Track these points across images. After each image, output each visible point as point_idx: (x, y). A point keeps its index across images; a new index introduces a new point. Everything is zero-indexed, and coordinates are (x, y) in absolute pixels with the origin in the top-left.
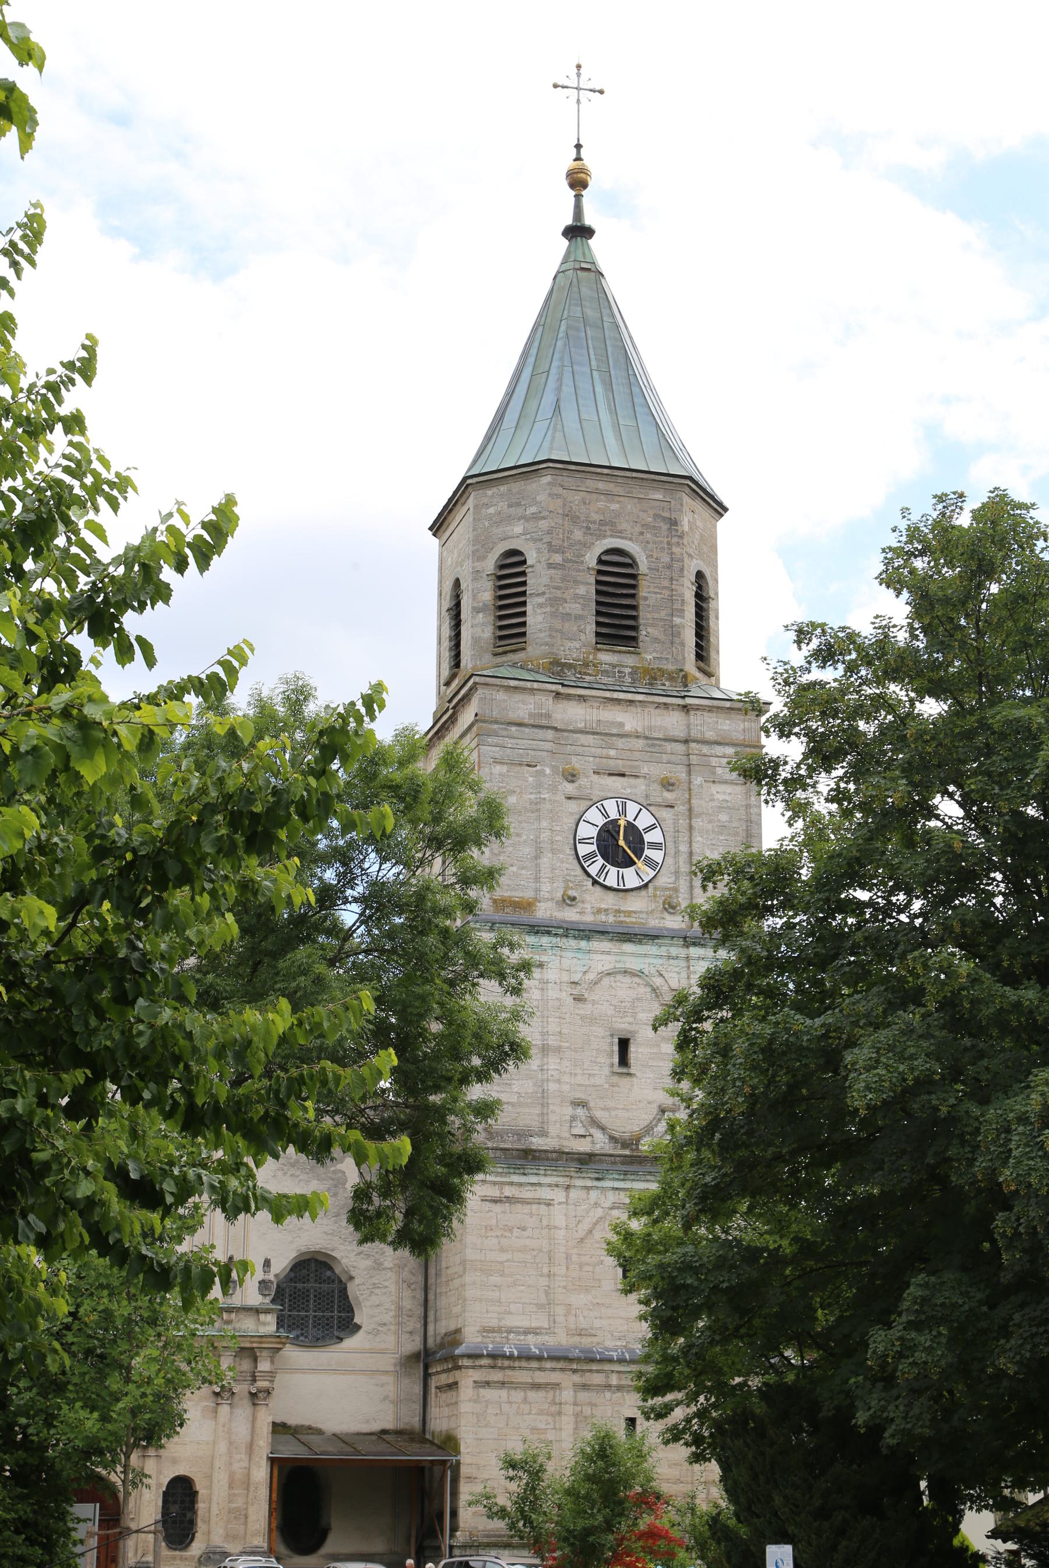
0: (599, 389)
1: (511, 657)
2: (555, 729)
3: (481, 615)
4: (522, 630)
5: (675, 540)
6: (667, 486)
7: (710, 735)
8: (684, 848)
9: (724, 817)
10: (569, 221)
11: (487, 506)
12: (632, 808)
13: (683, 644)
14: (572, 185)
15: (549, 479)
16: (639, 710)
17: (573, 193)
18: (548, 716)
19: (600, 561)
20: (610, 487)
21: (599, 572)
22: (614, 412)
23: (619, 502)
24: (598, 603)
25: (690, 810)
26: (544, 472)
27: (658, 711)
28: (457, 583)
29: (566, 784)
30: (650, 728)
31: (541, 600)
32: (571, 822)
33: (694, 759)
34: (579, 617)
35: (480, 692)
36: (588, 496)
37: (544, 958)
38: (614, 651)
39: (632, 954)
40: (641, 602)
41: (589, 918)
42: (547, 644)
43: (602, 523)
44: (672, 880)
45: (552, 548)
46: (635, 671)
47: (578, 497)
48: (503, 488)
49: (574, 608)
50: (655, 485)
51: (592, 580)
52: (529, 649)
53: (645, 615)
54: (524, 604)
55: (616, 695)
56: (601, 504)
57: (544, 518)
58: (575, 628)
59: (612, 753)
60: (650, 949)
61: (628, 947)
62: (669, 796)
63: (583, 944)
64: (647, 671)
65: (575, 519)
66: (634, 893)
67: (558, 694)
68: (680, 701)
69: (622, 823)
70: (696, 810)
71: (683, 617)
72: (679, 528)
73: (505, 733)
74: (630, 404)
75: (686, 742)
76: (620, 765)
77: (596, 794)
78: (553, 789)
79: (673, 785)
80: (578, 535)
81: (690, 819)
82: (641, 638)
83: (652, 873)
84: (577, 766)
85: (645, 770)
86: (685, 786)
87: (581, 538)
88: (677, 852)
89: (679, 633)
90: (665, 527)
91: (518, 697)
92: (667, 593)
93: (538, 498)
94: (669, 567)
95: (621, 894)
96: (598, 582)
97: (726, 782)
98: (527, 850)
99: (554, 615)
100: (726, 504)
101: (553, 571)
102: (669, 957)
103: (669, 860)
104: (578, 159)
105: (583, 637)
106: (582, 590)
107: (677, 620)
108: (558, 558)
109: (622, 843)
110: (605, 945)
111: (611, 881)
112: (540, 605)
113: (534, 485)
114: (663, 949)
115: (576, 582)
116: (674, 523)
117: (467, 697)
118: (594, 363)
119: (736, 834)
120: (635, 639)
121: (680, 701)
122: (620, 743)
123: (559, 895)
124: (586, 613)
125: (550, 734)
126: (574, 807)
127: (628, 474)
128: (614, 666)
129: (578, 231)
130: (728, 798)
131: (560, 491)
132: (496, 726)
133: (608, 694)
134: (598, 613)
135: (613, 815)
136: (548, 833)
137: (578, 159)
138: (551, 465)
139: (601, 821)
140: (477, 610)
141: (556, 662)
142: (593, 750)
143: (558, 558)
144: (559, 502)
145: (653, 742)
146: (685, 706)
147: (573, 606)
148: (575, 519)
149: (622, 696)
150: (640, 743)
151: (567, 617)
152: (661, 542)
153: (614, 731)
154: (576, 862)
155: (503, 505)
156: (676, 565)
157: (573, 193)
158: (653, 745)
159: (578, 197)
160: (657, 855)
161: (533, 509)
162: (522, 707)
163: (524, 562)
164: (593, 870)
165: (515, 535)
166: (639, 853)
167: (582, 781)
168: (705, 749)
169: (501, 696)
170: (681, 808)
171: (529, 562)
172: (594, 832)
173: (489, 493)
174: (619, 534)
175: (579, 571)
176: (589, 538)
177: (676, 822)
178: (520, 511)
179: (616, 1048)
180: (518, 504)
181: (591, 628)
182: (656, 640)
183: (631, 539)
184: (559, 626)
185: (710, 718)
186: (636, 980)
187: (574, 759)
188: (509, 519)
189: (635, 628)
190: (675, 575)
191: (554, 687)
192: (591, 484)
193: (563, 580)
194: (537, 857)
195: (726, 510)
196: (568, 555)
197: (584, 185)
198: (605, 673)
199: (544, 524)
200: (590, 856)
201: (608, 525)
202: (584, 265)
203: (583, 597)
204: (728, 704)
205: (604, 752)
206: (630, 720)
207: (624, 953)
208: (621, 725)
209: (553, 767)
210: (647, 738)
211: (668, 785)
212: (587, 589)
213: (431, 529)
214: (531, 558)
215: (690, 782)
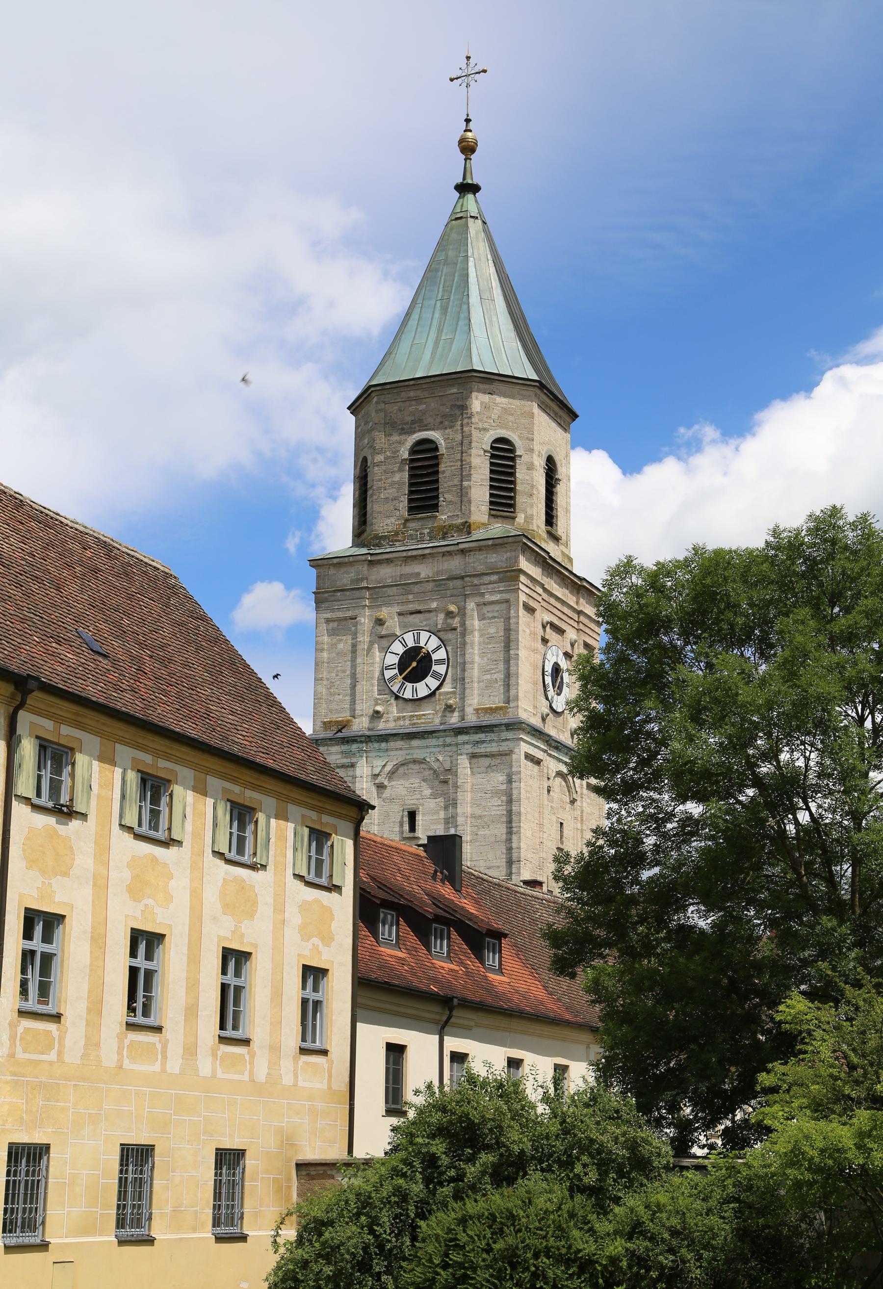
0: (437, 315)
6: (459, 381)
7: (481, 568)
12: (424, 635)
16: (431, 560)
19: (413, 451)
21: (412, 461)
22: (440, 331)
23: (425, 403)
27: (445, 558)
34: (394, 499)
37: (354, 760)
38: (419, 519)
39: (418, 748)
41: (391, 725)
43: (413, 422)
56: (412, 409)
58: (392, 508)
60: (432, 741)
61: (415, 743)
63: (383, 745)
66: (426, 701)
71: (470, 480)
72: (469, 411)
73: (332, 598)
83: (438, 683)
89: (467, 493)
91: (343, 570)
95: (417, 703)
102: (444, 746)
106: (397, 478)
110: (399, 743)
111: (408, 694)
114: (441, 739)
122: (416, 589)
123: (371, 711)
127: (428, 380)
131: (382, 406)
132: (326, 595)
142: (397, 598)
144: (382, 414)
150: (431, 585)
157: (464, 157)
160: (441, 669)
164: (395, 689)
168: (476, 581)
169: (332, 571)
172: (395, 660)
176: (403, 437)
179: (406, 819)
181: (404, 504)
182: (451, 502)
183: (433, 429)
185: (480, 556)
186: (423, 766)
191: (363, 558)
196: (388, 454)
203: (398, 483)
204: (490, 542)
207: (411, 748)
208: (418, 574)
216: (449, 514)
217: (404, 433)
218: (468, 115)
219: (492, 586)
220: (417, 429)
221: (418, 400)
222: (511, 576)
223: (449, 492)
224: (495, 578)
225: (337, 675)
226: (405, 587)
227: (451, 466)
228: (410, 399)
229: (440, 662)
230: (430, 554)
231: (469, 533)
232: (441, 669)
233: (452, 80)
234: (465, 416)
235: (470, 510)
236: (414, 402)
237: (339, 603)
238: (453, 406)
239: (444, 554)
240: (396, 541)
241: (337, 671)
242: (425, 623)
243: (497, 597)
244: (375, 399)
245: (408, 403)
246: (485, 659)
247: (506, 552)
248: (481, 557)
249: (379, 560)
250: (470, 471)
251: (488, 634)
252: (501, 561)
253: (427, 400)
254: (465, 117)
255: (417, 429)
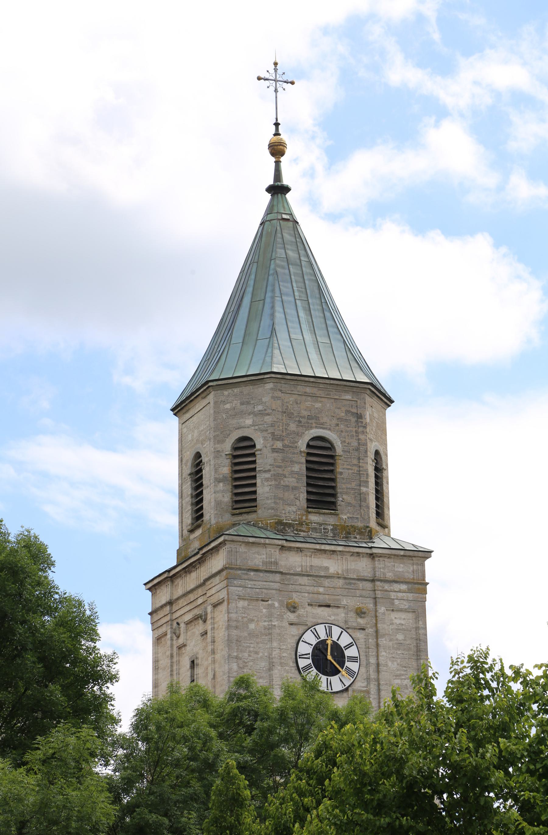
0: (302, 314)
1: (245, 517)
2: (281, 573)
3: (221, 484)
4: (253, 497)
5: (361, 429)
7: (390, 575)
8: (373, 660)
9: (400, 637)
10: (271, 182)
11: (224, 403)
12: (336, 631)
13: (368, 507)
14: (273, 154)
15: (271, 385)
16: (339, 557)
17: (273, 159)
18: (276, 563)
19: (308, 446)
20: (314, 391)
21: (308, 454)
23: (321, 402)
24: (308, 477)
25: (377, 632)
26: (268, 380)
27: (352, 558)
28: (198, 455)
29: (289, 614)
30: (347, 571)
31: (267, 475)
32: (293, 641)
33: (379, 594)
34: (295, 488)
35: (228, 546)
36: (299, 398)
38: (320, 513)
40: (338, 476)
42: (272, 508)
43: (309, 417)
44: (365, 684)
45: (275, 437)
46: (335, 527)
47: (292, 399)
48: (236, 390)
49: (291, 481)
50: (346, 389)
51: (303, 460)
52: (259, 512)
53: (341, 486)
54: (254, 477)
55: (323, 547)
56: (308, 404)
57: (268, 414)
59: (321, 590)
62: (361, 621)
64: (343, 528)
65: (290, 415)
66: (338, 695)
67: (283, 546)
68: (368, 551)
69: (329, 642)
70: (381, 631)
71: (367, 487)
72: (363, 420)
74: (324, 326)
75: (373, 581)
76: (326, 599)
77: (310, 621)
78: (281, 617)
79: (364, 613)
80: (293, 427)
81: (377, 638)
82: (339, 503)
84: (297, 600)
85: (344, 602)
86: (373, 613)
87: (295, 429)
88: (368, 664)
90: (353, 420)
91: (254, 549)
92: (356, 469)
93: (264, 400)
94: (357, 449)
96: (307, 462)
97: (401, 610)
98: (263, 664)
99: (277, 487)
100: (393, 398)
101: (276, 454)
103: (363, 670)
104: (277, 134)
105: (298, 503)
106: (296, 468)
107: (364, 489)
108: (279, 445)
109: (329, 657)
112: (267, 480)
113: (260, 390)
115: (292, 462)
116: (359, 417)
117: (216, 549)
118: (296, 294)
119: (409, 649)
120: (334, 503)
121: (368, 551)
122: (327, 582)
124: (299, 485)
125: (278, 577)
126: (295, 631)
127: (327, 381)
128: (321, 525)
129: (278, 190)
130: (403, 622)
131: (279, 394)
132: (239, 572)
133: (318, 547)
134: (308, 485)
135: (323, 636)
136: (278, 651)
137: (277, 134)
138: (273, 376)
139: (314, 641)
140: (218, 481)
141: (280, 523)
142: (308, 588)
143: (279, 445)
145: (350, 581)
146: (371, 554)
147: (291, 480)
148: (290, 415)
149: (327, 547)
150: (341, 582)
151: (286, 488)
152: (351, 431)
153: (322, 574)
154: (297, 672)
155: (236, 403)
156: (362, 448)
158: (350, 584)
159: (278, 164)
160: (354, 666)
161: (260, 407)
162: (258, 557)
163: (254, 446)
165: (247, 426)
166: (342, 665)
167: (301, 611)
168: (387, 586)
169: (242, 549)
170: (371, 631)
171: (258, 447)
173: (226, 393)
174: (321, 426)
175: (294, 453)
176: (300, 429)
177: (366, 640)
178: (250, 408)
180: (248, 403)
181: (303, 496)
182: (349, 504)
183: (330, 429)
184: (281, 495)
185: (389, 563)
187: (294, 595)
188: (242, 414)
189: (334, 495)
190: (362, 456)
191: (280, 542)
192: (301, 389)
193: (283, 460)
194: (270, 669)
195: (392, 402)
197: (282, 154)
198: (315, 530)
199: (268, 419)
200: (308, 667)
201: (314, 419)
202: (285, 216)
203: (297, 473)
204: (402, 553)
205: (316, 589)
206: (333, 566)
208: (327, 568)
209: (280, 602)
210: (345, 578)
211: (360, 613)
212: (300, 467)
213: (172, 410)
214: (259, 443)
215: (376, 611)
216: (348, 515)
217: (302, 426)
218: (277, 119)
219: (401, 594)
220: (314, 425)
221: (313, 396)
222: (419, 589)
223: (346, 493)
224: (404, 587)
225: (250, 656)
226: (316, 579)
227: (348, 469)
228: (306, 394)
229: (353, 659)
230: (340, 551)
231: (371, 538)
232: (354, 666)
233: (259, 79)
234: (360, 424)
235: (368, 515)
236: (309, 398)
237: (251, 582)
238: (347, 412)
239: (353, 554)
240: (301, 531)
241: (250, 652)
242: (333, 618)
243: (405, 605)
244: (269, 386)
245: (304, 397)
246: (395, 663)
247: (413, 564)
248: (389, 565)
249: (290, 547)
250: (367, 478)
251: (397, 639)
252: (408, 572)
253: (323, 399)
254: (275, 121)
255: (314, 425)
